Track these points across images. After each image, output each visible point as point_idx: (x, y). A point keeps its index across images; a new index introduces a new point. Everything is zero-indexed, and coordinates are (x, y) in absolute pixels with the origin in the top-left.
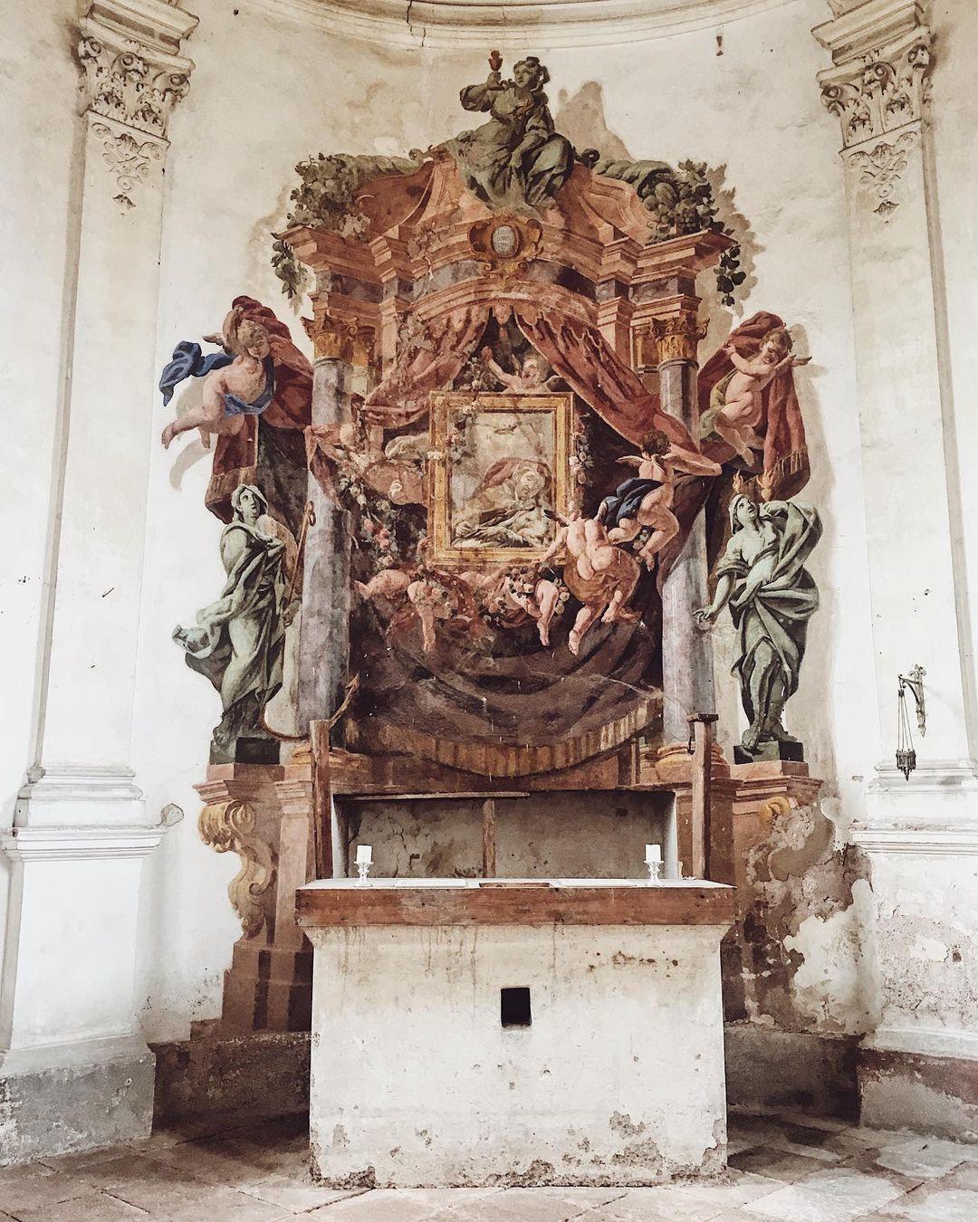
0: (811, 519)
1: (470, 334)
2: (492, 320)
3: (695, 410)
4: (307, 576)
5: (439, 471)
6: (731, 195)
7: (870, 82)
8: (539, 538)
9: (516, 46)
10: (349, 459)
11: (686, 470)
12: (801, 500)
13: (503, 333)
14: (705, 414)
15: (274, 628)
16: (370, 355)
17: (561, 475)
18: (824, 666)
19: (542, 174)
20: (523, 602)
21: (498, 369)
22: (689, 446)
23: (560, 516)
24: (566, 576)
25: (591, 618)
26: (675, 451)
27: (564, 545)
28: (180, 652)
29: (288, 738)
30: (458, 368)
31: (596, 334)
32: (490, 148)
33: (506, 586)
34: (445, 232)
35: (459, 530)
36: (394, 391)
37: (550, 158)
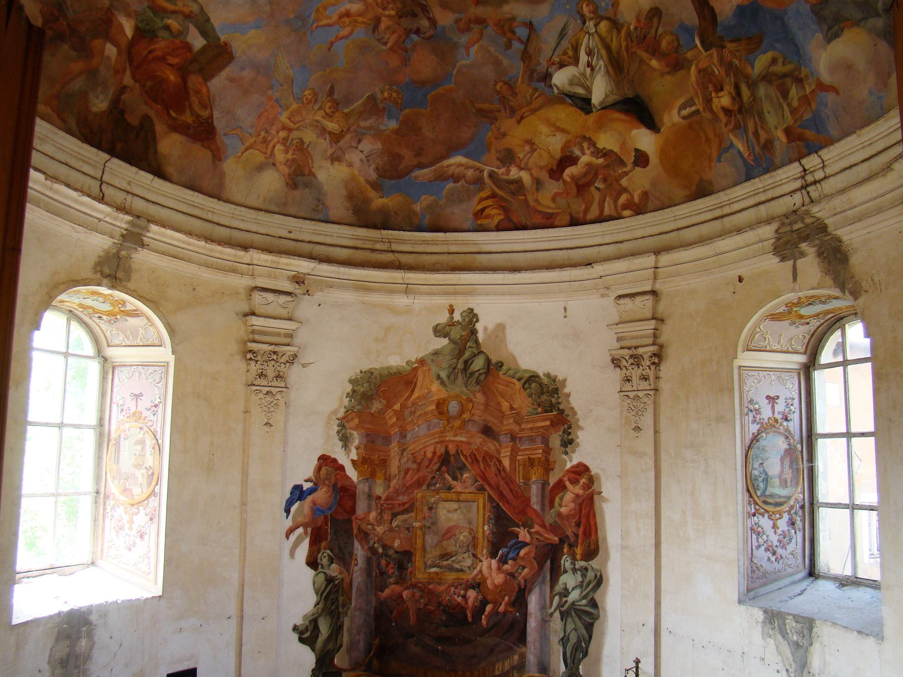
0: (598, 574)
1: (436, 459)
2: (447, 452)
3: (547, 508)
4: (354, 591)
5: (419, 532)
6: (568, 395)
7: (632, 364)
8: (469, 568)
9: (461, 304)
10: (374, 530)
11: (542, 539)
12: (594, 563)
13: (452, 459)
14: (552, 511)
15: (338, 618)
16: (385, 474)
17: (480, 536)
18: (600, 647)
19: (474, 372)
20: (460, 599)
21: (450, 478)
22: (543, 526)
23: (479, 556)
24: (481, 587)
25: (493, 609)
26: (536, 528)
27: (481, 571)
28: (295, 636)
29: (345, 670)
30: (430, 478)
31: (500, 462)
32: (448, 357)
33: (452, 591)
34: (423, 405)
35: (429, 563)
36: (397, 492)
37: (478, 364)
